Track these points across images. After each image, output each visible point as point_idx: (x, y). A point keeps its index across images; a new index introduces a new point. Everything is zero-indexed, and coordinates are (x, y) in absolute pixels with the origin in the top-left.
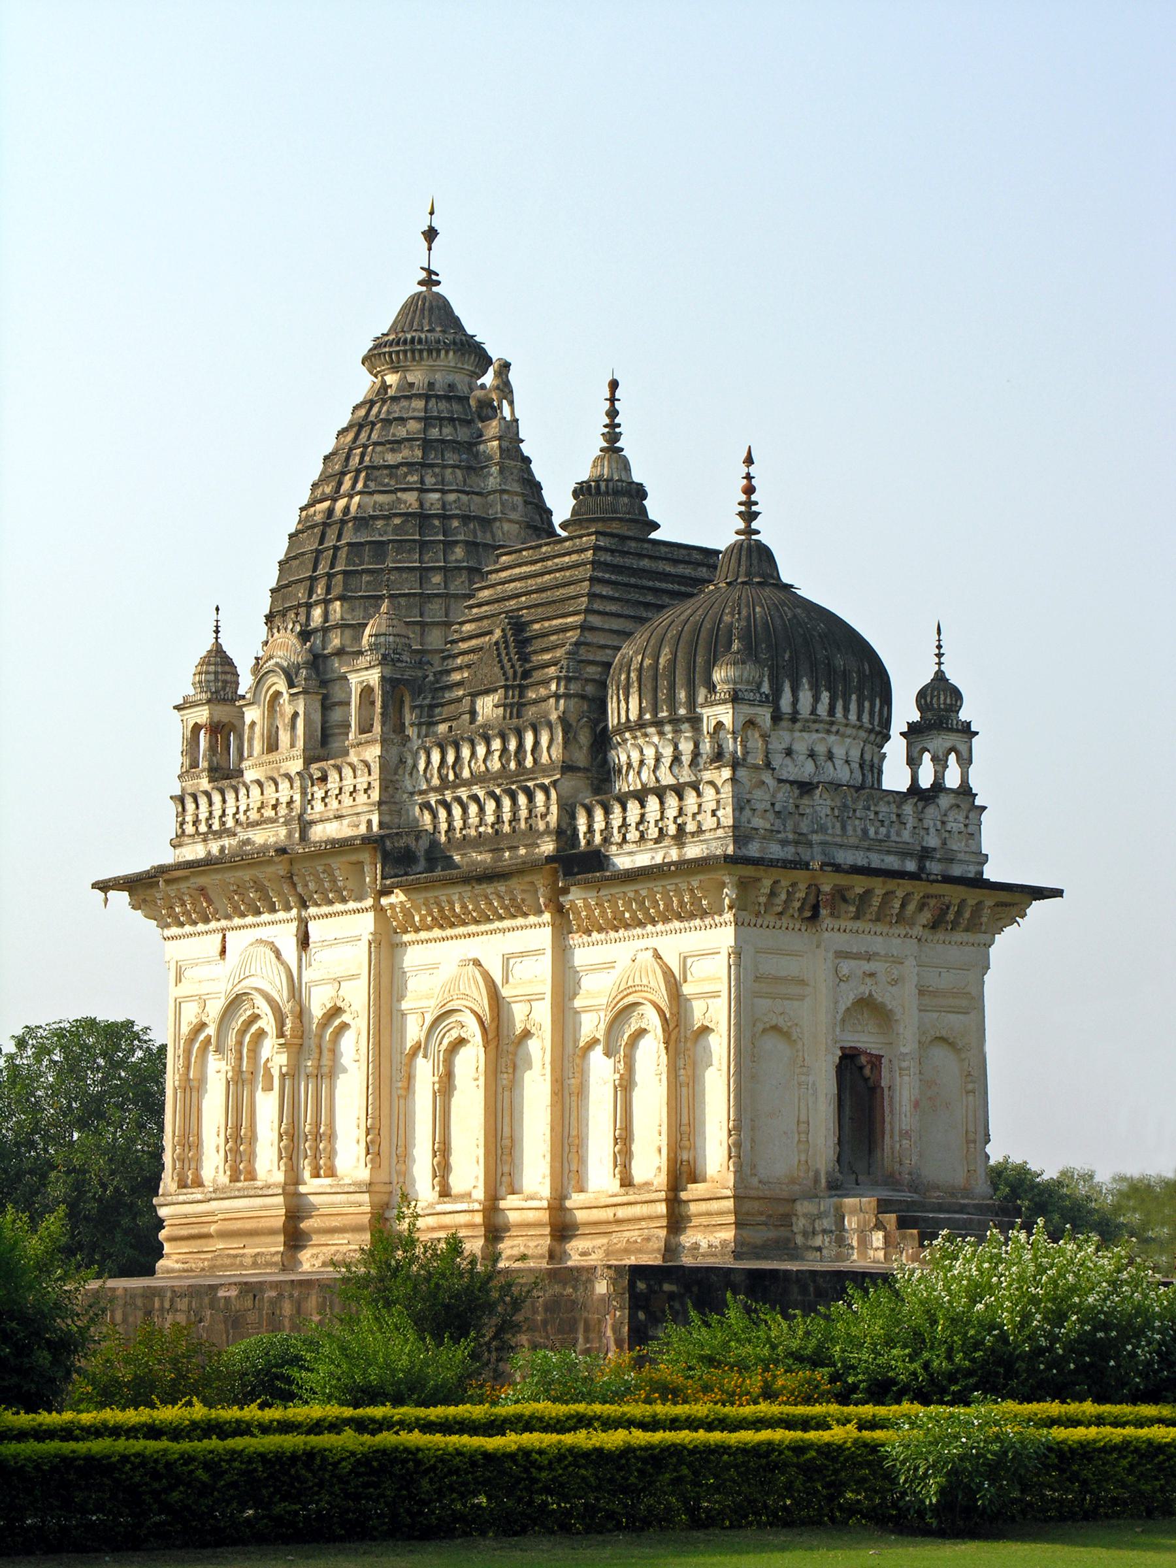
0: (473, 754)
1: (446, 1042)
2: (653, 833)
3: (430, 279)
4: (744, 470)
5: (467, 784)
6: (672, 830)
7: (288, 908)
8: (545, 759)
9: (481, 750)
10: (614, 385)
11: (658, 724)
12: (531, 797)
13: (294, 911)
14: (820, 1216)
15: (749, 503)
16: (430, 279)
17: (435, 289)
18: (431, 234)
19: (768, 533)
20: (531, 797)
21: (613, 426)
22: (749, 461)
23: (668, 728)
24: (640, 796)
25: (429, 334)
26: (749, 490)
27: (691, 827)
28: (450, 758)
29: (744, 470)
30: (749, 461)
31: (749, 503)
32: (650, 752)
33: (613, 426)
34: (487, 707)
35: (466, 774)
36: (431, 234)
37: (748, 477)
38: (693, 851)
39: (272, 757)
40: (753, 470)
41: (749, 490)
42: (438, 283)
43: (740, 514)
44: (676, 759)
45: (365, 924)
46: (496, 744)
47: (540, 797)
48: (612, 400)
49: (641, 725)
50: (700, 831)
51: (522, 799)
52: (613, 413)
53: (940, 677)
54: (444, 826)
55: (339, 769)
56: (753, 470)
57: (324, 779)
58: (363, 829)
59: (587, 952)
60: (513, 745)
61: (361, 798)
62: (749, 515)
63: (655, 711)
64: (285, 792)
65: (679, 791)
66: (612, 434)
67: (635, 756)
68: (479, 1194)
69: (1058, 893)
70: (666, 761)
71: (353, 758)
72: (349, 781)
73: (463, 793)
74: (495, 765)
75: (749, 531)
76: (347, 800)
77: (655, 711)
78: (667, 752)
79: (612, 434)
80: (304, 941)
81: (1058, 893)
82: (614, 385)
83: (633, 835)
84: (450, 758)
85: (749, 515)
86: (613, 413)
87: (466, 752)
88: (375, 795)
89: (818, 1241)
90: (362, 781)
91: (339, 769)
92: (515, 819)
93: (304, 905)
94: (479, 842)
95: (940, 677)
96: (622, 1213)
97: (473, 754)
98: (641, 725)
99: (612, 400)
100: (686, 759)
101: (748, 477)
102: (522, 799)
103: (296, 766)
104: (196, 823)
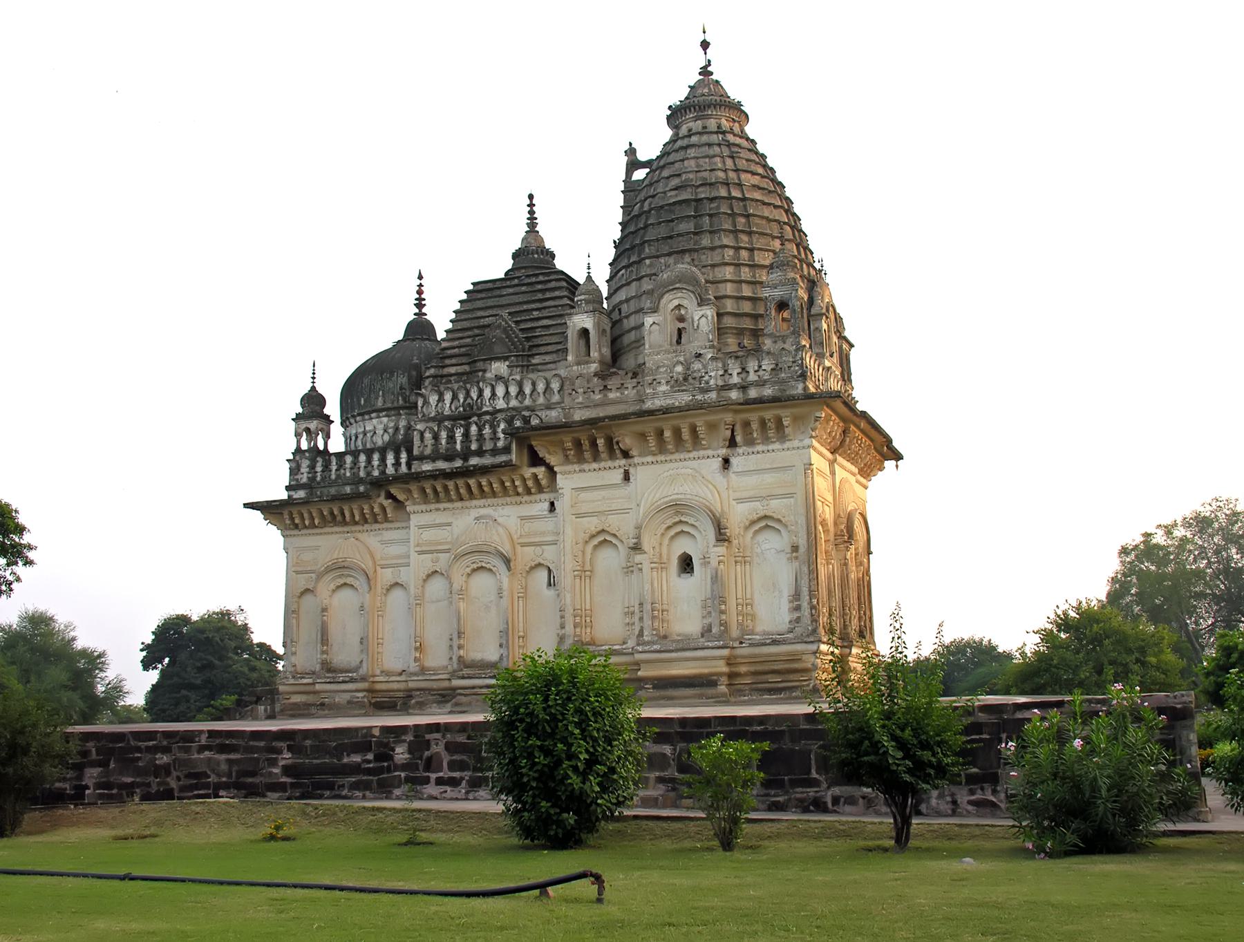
10: (531, 197)
16: (705, 71)
18: (705, 45)
22: (420, 277)
26: (420, 292)
30: (420, 277)
36: (705, 45)
37: (421, 285)
40: (418, 282)
41: (420, 292)
48: (531, 205)
53: (313, 388)
56: (418, 282)
62: (420, 304)
69: (247, 506)
75: (420, 314)
81: (247, 506)
82: (531, 197)
85: (420, 304)
86: (532, 212)
95: (313, 388)
101: (421, 285)
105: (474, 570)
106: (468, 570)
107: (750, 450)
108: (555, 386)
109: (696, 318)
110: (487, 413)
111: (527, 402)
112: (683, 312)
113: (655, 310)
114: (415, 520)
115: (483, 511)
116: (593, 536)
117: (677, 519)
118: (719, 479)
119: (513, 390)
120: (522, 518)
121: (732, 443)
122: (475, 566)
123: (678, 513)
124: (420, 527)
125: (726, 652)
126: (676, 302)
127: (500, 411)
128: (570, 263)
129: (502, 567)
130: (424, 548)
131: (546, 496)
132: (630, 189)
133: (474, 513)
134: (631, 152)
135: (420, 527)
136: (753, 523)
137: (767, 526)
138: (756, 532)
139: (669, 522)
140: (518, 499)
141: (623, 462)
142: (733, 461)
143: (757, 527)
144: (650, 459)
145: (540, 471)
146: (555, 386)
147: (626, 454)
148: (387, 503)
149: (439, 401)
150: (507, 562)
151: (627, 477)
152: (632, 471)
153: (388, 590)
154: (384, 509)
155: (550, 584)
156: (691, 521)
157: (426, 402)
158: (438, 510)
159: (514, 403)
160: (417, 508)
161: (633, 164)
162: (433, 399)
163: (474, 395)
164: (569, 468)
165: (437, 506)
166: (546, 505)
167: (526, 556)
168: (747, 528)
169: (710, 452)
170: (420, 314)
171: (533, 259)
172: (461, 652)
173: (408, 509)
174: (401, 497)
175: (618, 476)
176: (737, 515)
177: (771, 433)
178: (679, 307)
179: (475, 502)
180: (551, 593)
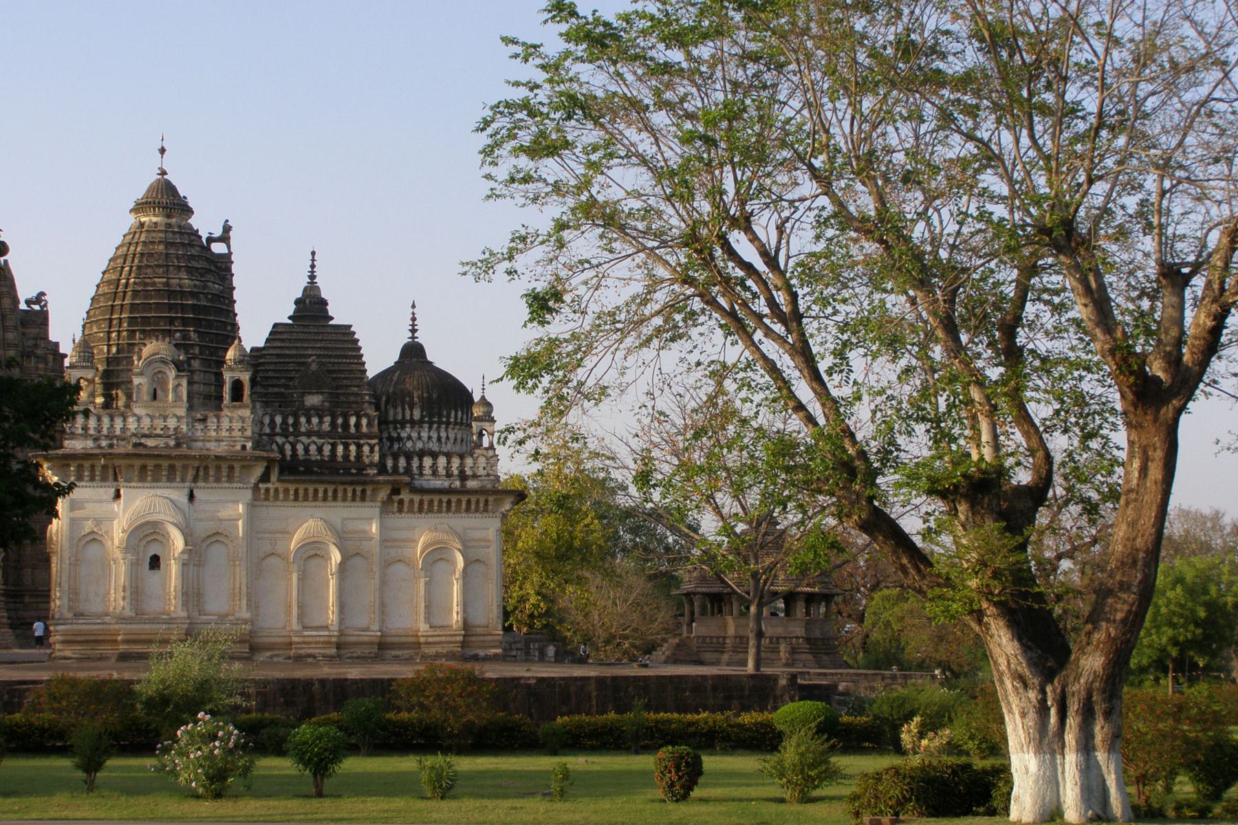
0: (309, 422)
1: (305, 556)
2: (442, 471)
3: (164, 173)
5: (309, 434)
6: (456, 472)
7: (183, 481)
8: (364, 429)
9: (315, 420)
10: (313, 253)
11: (431, 424)
12: (359, 447)
13: (187, 484)
14: (515, 642)
15: (413, 325)
18: (163, 151)
19: (421, 338)
20: (359, 447)
22: (413, 306)
23: (435, 426)
24: (434, 456)
25: (166, 200)
26: (414, 319)
27: (469, 472)
28: (291, 421)
30: (413, 306)
32: (424, 435)
33: (312, 272)
34: (313, 400)
35: (303, 429)
36: (163, 151)
38: (471, 484)
39: (155, 404)
41: (414, 319)
44: (439, 439)
45: (248, 495)
46: (328, 419)
47: (366, 449)
48: (313, 260)
49: (421, 422)
50: (475, 476)
51: (353, 448)
52: (313, 266)
54: (289, 453)
55: (218, 418)
57: (204, 420)
58: (238, 447)
59: (402, 522)
60: (340, 421)
61: (237, 433)
62: (414, 331)
63: (431, 416)
64: (172, 423)
65: (462, 457)
66: (312, 277)
67: (414, 435)
68: (335, 627)
70: (435, 440)
71: (226, 412)
72: (225, 424)
73: (304, 439)
74: (326, 427)
75: (413, 338)
76: (224, 434)
77: (431, 416)
78: (434, 435)
79: (312, 277)
80: (191, 497)
82: (313, 253)
83: (427, 471)
84: (291, 421)
85: (414, 331)
86: (313, 266)
87: (303, 420)
88: (249, 433)
89: (514, 653)
90: (237, 425)
91: (218, 418)
92: (346, 456)
93: (195, 479)
94: (321, 464)
96: (430, 640)
97: (309, 422)
98: (421, 422)
99: (313, 260)
100: (443, 440)
102: (353, 448)
103: (182, 412)
104: (85, 428)
170: (413, 338)
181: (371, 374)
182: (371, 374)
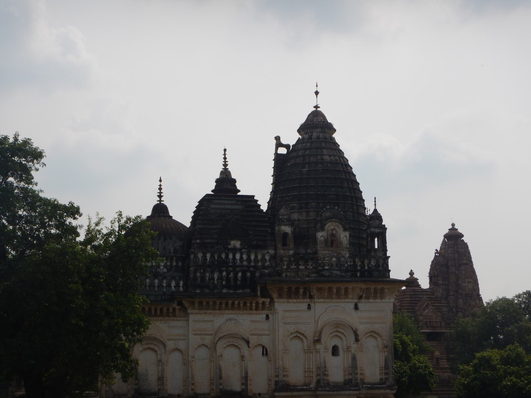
3: (316, 107)
4: (159, 183)
10: (225, 150)
15: (160, 193)
17: (318, 109)
18: (317, 93)
21: (225, 162)
22: (160, 181)
26: (160, 189)
29: (159, 183)
30: (160, 181)
31: (160, 193)
33: (225, 162)
36: (317, 93)
37: (160, 185)
41: (160, 189)
42: (319, 107)
43: (158, 196)
48: (225, 154)
52: (225, 158)
62: (160, 196)
66: (225, 165)
75: (160, 201)
79: (225, 165)
82: (225, 150)
85: (160, 196)
86: (225, 158)
99: (225, 154)
101: (160, 185)
105: (228, 346)
106: (225, 345)
107: (367, 301)
108: (267, 257)
109: (342, 236)
110: (231, 266)
111: (252, 264)
112: (334, 232)
113: (323, 229)
114: (192, 317)
115: (231, 316)
116: (292, 334)
117: (336, 330)
118: (353, 312)
119: (245, 257)
120: (252, 321)
121: (360, 297)
122: (229, 344)
123: (338, 327)
124: (194, 321)
125: (358, 392)
126: (332, 227)
127: (238, 266)
128: (244, 188)
129: (244, 345)
130: (198, 332)
131: (265, 312)
132: (278, 158)
133: (226, 317)
134: (278, 138)
135: (194, 321)
136: (367, 333)
137: (371, 335)
138: (366, 337)
139: (332, 331)
140: (251, 312)
141: (308, 300)
142: (360, 305)
143: (367, 336)
144: (322, 300)
145: (267, 300)
146: (267, 257)
147: (311, 297)
148: (177, 308)
149: (203, 257)
150: (248, 342)
151: (309, 307)
152: (312, 305)
153: (171, 352)
154: (174, 309)
155: (263, 354)
156: (342, 331)
157: (196, 256)
158: (205, 313)
159: (245, 263)
160: (194, 311)
161: (279, 144)
162: (200, 255)
163: (223, 256)
164: (281, 300)
165: (205, 311)
166: (264, 316)
167: (253, 340)
168: (363, 336)
169: (350, 300)
170: (160, 201)
171: (226, 183)
172: (221, 387)
173: (189, 311)
174: (187, 305)
175: (305, 306)
176: (362, 329)
177: (378, 295)
178: (334, 229)
179: (227, 311)
180: (264, 359)
181: (188, 224)
182: (188, 224)
